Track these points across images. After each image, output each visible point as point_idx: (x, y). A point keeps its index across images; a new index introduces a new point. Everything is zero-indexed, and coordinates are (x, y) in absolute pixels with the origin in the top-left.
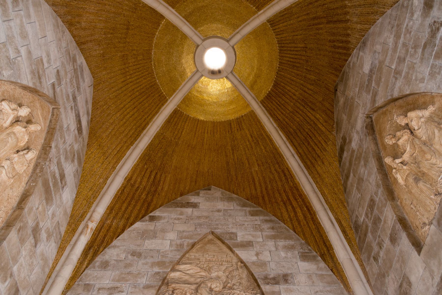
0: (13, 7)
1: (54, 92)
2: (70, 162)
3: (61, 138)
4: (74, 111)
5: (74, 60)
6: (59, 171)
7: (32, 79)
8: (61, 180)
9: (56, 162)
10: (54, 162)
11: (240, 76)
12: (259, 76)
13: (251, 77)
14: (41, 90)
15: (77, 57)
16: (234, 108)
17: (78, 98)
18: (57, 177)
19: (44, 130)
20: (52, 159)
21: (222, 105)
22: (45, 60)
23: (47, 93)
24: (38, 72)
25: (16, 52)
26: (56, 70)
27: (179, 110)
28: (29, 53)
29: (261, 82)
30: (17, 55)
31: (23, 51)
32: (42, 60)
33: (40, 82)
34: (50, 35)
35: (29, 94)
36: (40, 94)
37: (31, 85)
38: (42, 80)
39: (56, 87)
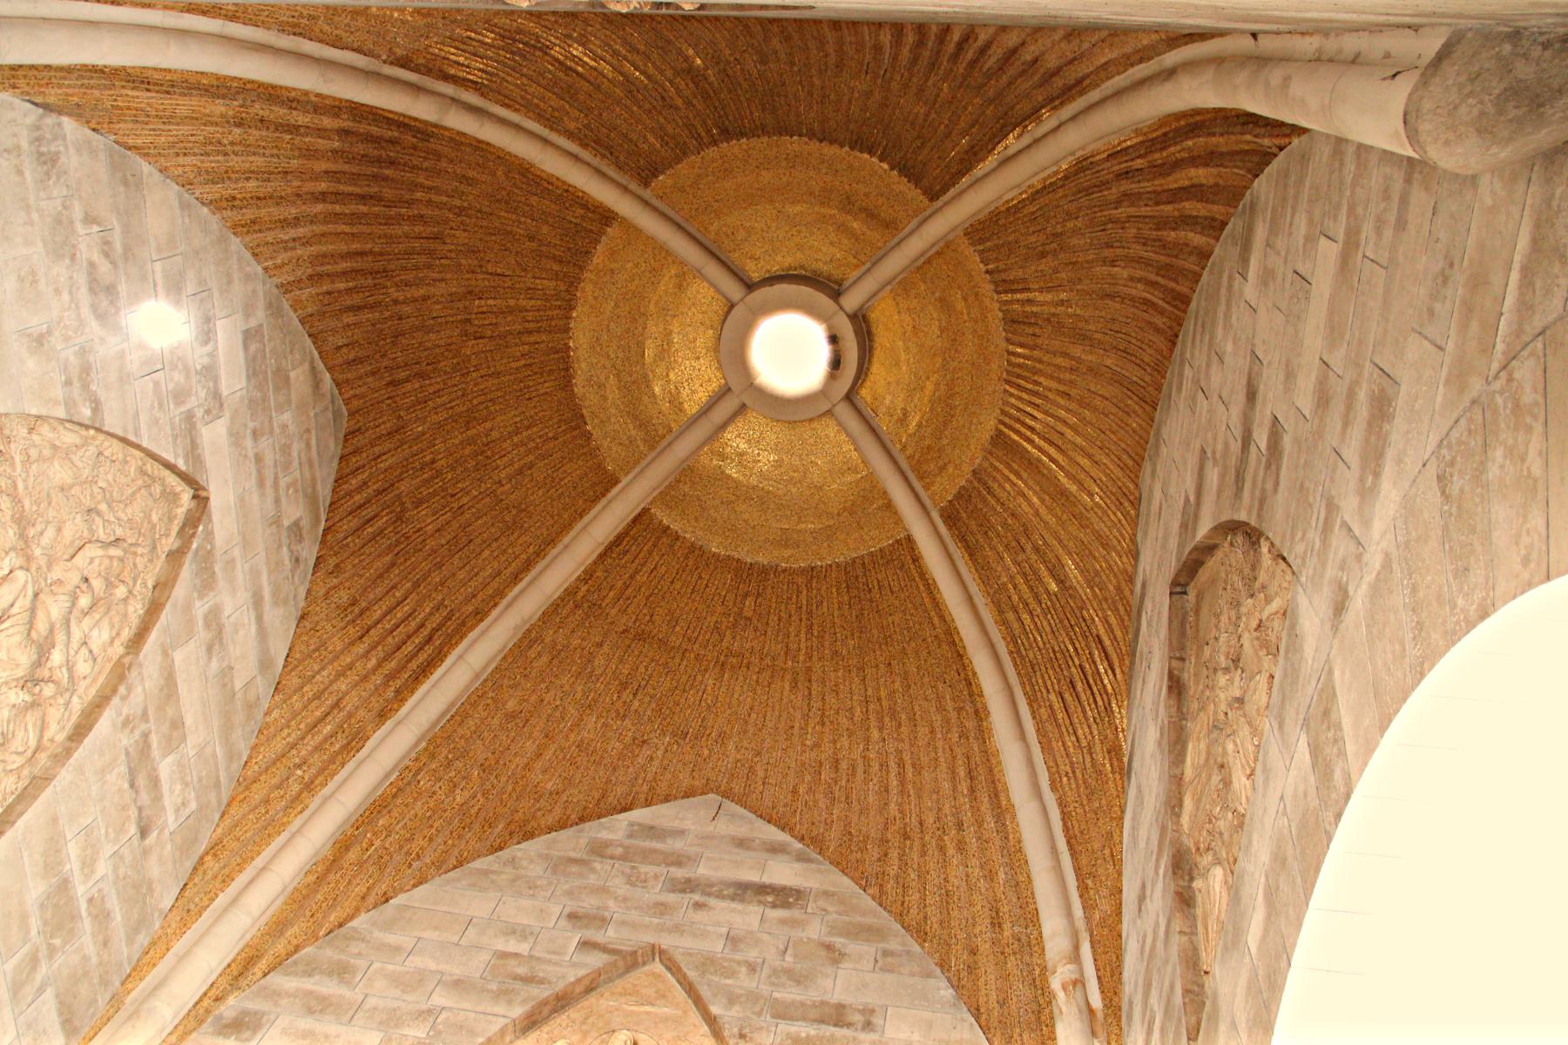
0: (347, 983)
1: (604, 949)
2: (830, 970)
3: (732, 974)
4: (712, 902)
5: (599, 850)
6: (804, 1019)
7: (510, 1002)
8: (836, 1025)
9: (768, 1018)
10: (761, 1028)
11: (855, 261)
12: (848, 198)
13: (855, 225)
14: (560, 986)
15: (605, 835)
16: (965, 299)
17: (703, 871)
18: (813, 1032)
19: (685, 1012)
20: (746, 1031)
21: (955, 340)
22: (512, 946)
23: (581, 972)
24: (517, 978)
25: (425, 1019)
26: (563, 923)
27: (950, 502)
28: (459, 985)
29: (866, 195)
30: (431, 1020)
31: (439, 999)
32: (504, 955)
33: (541, 981)
34: (477, 905)
35: (563, 1017)
36: (578, 989)
37: (518, 1011)
38: (541, 975)
39: (598, 937)
